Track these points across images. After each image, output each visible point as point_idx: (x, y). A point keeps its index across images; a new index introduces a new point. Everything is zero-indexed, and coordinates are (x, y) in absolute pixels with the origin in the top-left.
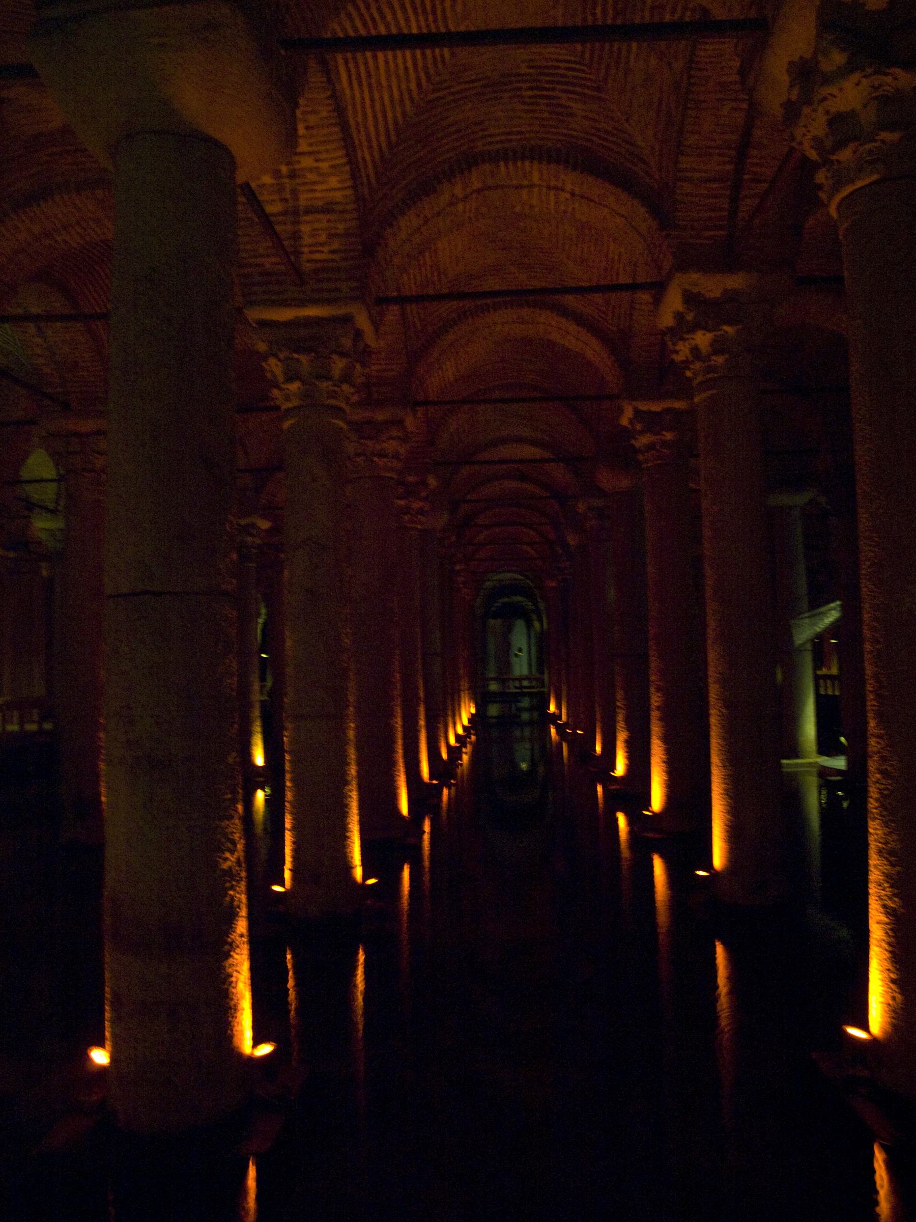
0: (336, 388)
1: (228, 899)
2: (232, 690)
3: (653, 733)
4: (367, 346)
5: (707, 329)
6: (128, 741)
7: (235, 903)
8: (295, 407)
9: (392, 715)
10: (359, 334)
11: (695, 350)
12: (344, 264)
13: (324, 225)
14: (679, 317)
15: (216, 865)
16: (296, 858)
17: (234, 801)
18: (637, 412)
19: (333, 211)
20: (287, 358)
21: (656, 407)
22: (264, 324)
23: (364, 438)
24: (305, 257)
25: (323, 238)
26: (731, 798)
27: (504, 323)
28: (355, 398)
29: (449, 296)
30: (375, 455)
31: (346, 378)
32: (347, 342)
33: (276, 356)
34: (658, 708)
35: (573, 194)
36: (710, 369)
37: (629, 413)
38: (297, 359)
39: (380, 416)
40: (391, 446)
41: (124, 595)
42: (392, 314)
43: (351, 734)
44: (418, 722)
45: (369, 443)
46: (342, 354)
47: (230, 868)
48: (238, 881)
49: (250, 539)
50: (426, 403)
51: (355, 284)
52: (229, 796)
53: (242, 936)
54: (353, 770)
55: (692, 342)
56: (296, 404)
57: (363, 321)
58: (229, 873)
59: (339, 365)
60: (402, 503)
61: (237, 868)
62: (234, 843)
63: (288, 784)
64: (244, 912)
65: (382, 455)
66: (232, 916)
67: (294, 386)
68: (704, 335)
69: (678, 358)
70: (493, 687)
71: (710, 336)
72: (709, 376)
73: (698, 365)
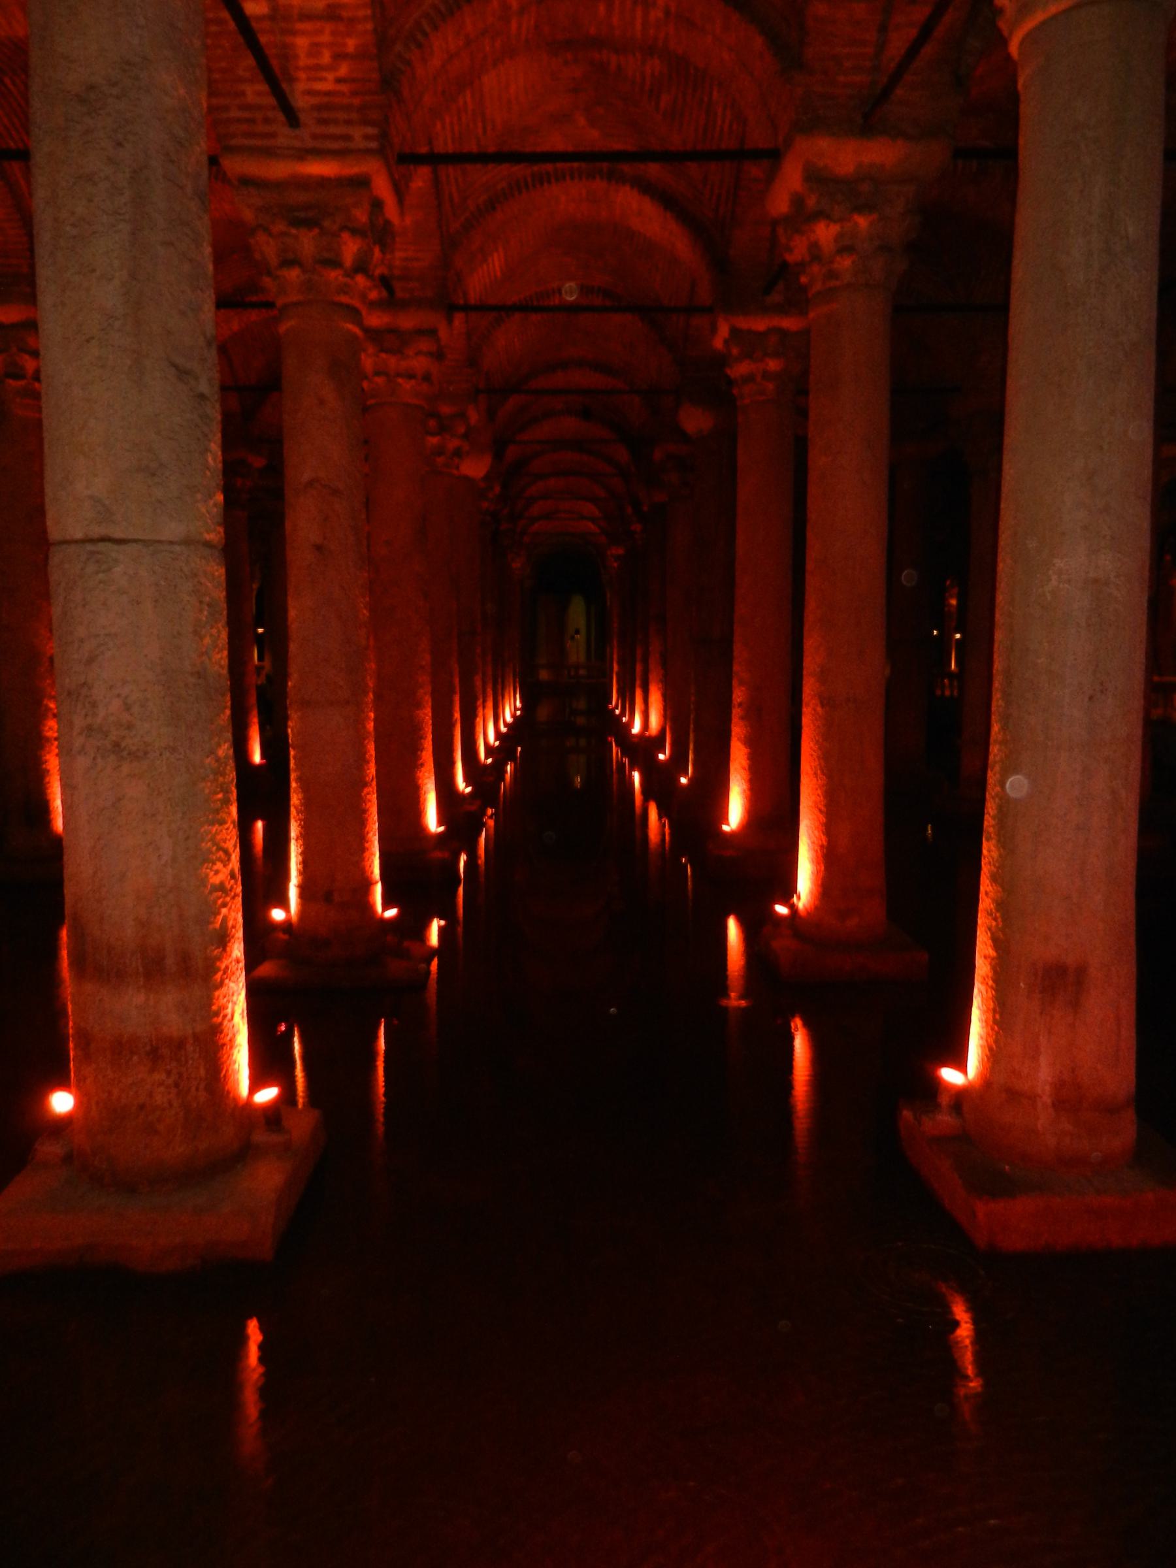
0: (348, 280)
1: (220, 917)
2: (221, 667)
3: (733, 734)
4: (388, 223)
5: (828, 217)
6: (90, 728)
7: (230, 924)
9: (418, 705)
10: (377, 204)
11: (814, 246)
12: (356, 101)
13: (326, 38)
14: (798, 201)
15: (203, 881)
16: (305, 871)
17: (226, 802)
18: (735, 332)
19: (340, 18)
21: (760, 324)
22: (247, 181)
24: (301, 86)
25: (326, 58)
26: (820, 811)
27: (567, 199)
28: (373, 295)
29: (500, 157)
30: (399, 375)
31: (361, 267)
32: (361, 215)
34: (740, 705)
35: (667, 13)
37: (724, 330)
39: (407, 321)
40: (420, 364)
41: (76, 542)
42: (420, 179)
43: (371, 726)
44: (452, 715)
45: (392, 362)
46: (355, 232)
47: (222, 883)
48: (233, 898)
50: (467, 308)
51: (370, 130)
52: (220, 796)
53: (238, 961)
54: (372, 770)
57: (382, 186)
58: (221, 888)
59: (350, 248)
60: (434, 440)
61: (232, 882)
62: (227, 854)
63: (294, 785)
64: (240, 934)
65: (411, 376)
66: (223, 939)
67: (294, 274)
68: (828, 226)
69: (791, 258)
70: (544, 675)
71: (835, 229)
73: (816, 268)
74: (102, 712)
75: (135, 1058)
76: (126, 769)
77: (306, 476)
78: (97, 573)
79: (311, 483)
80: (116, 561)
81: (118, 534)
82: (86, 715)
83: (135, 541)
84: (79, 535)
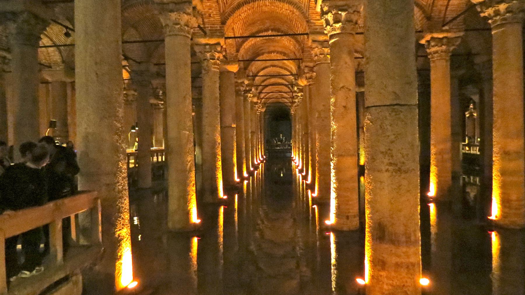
8: (337, 34)
20: (335, 14)
21: (441, 36)
23: (324, 47)
33: (331, 13)
36: (505, 19)
38: (341, 14)
41: (388, 106)
49: (242, 88)
55: (497, 8)
56: (338, 32)
67: (338, 25)
71: (507, 5)
72: (504, 22)
73: (498, 18)
74: (395, 158)
75: (402, 270)
76: (403, 176)
77: (341, 85)
78: (396, 115)
79: (343, 87)
80: (401, 112)
81: (401, 103)
82: (389, 160)
83: (406, 105)
84: (388, 104)
